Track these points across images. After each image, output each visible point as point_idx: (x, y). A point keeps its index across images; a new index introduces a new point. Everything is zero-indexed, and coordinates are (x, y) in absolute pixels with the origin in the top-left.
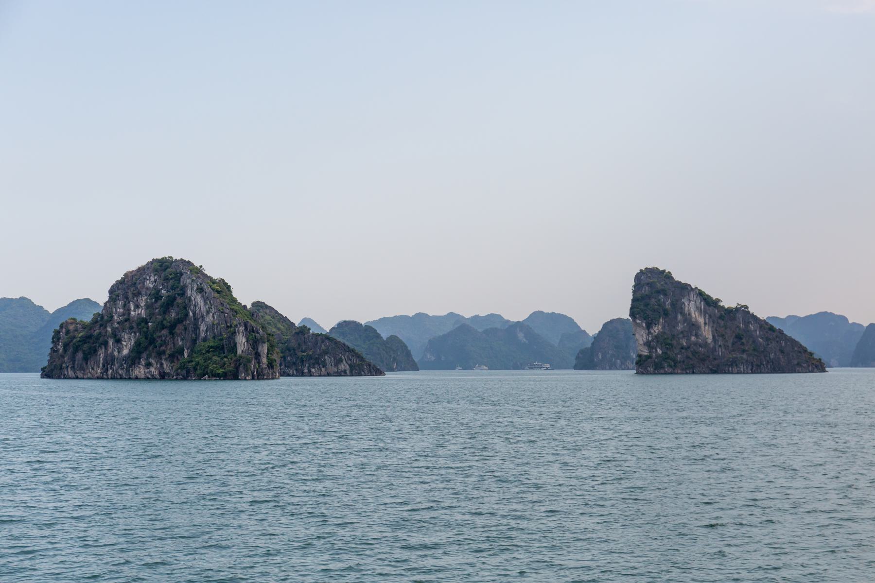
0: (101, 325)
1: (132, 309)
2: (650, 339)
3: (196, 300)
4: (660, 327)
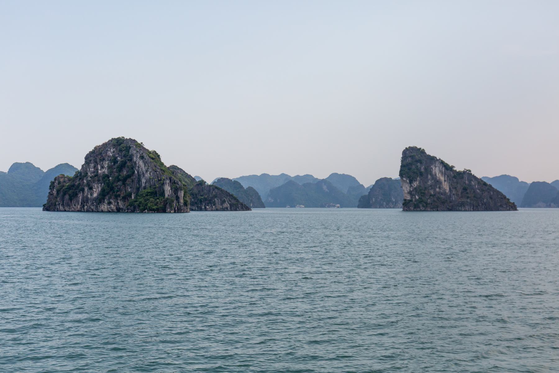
0: (80, 179)
1: (99, 169)
2: (411, 190)
3: (139, 164)
4: (418, 182)
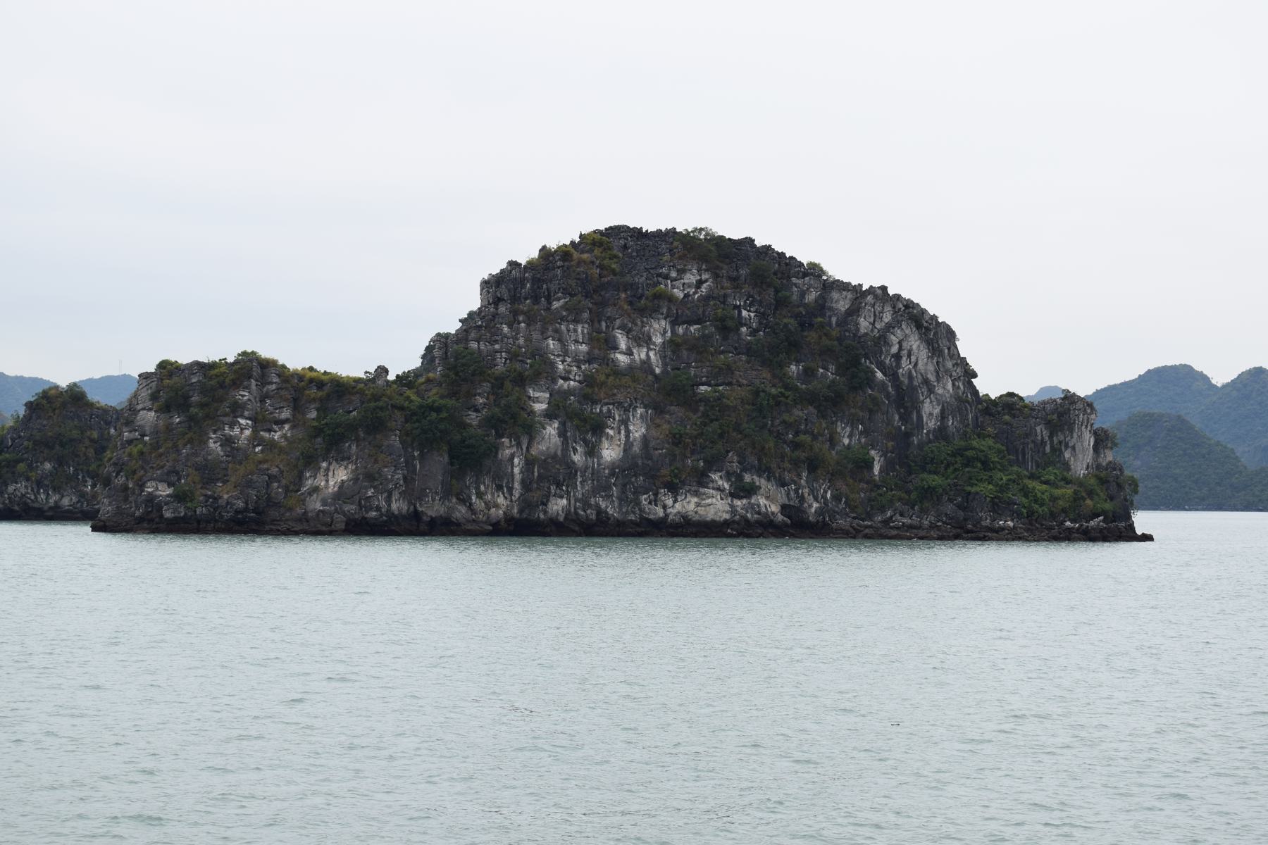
1: (623, 346)
3: (904, 344)
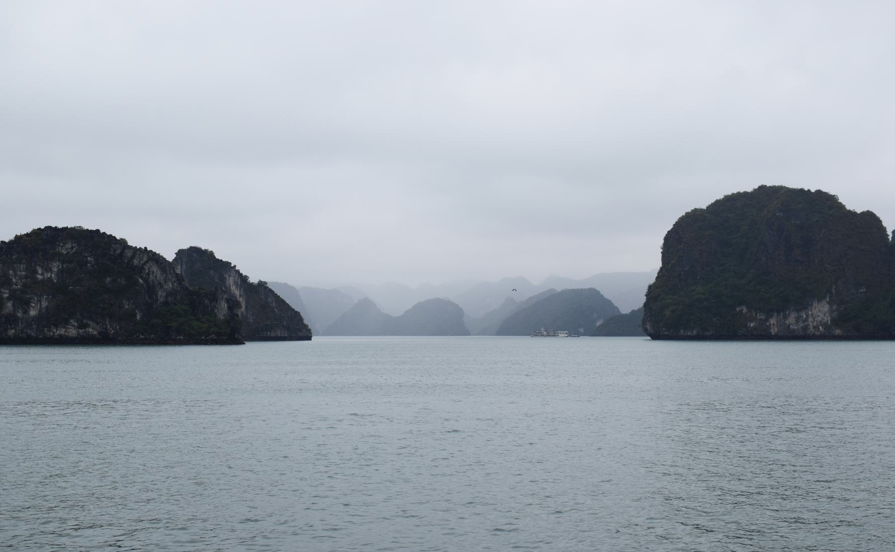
1: (40, 272)
